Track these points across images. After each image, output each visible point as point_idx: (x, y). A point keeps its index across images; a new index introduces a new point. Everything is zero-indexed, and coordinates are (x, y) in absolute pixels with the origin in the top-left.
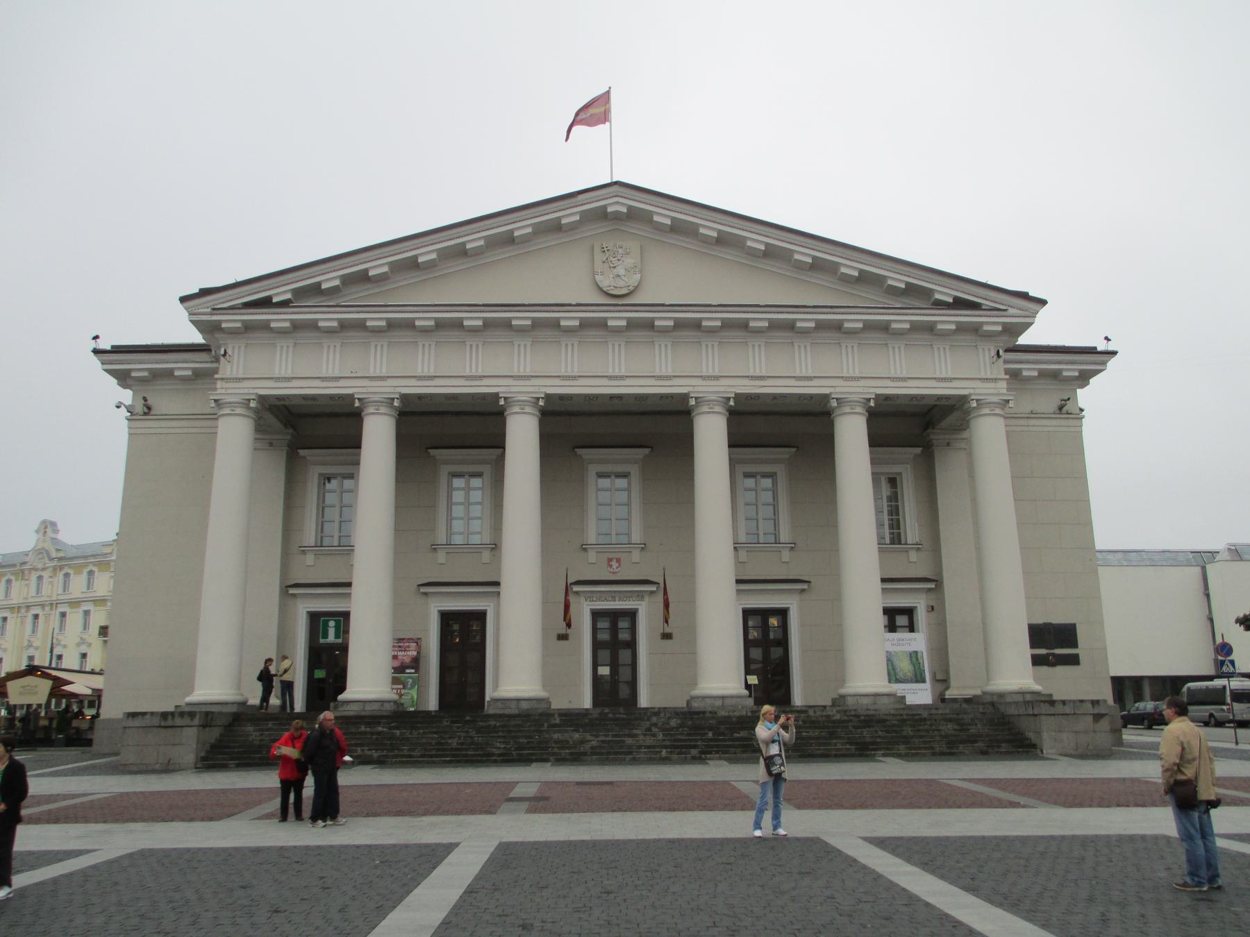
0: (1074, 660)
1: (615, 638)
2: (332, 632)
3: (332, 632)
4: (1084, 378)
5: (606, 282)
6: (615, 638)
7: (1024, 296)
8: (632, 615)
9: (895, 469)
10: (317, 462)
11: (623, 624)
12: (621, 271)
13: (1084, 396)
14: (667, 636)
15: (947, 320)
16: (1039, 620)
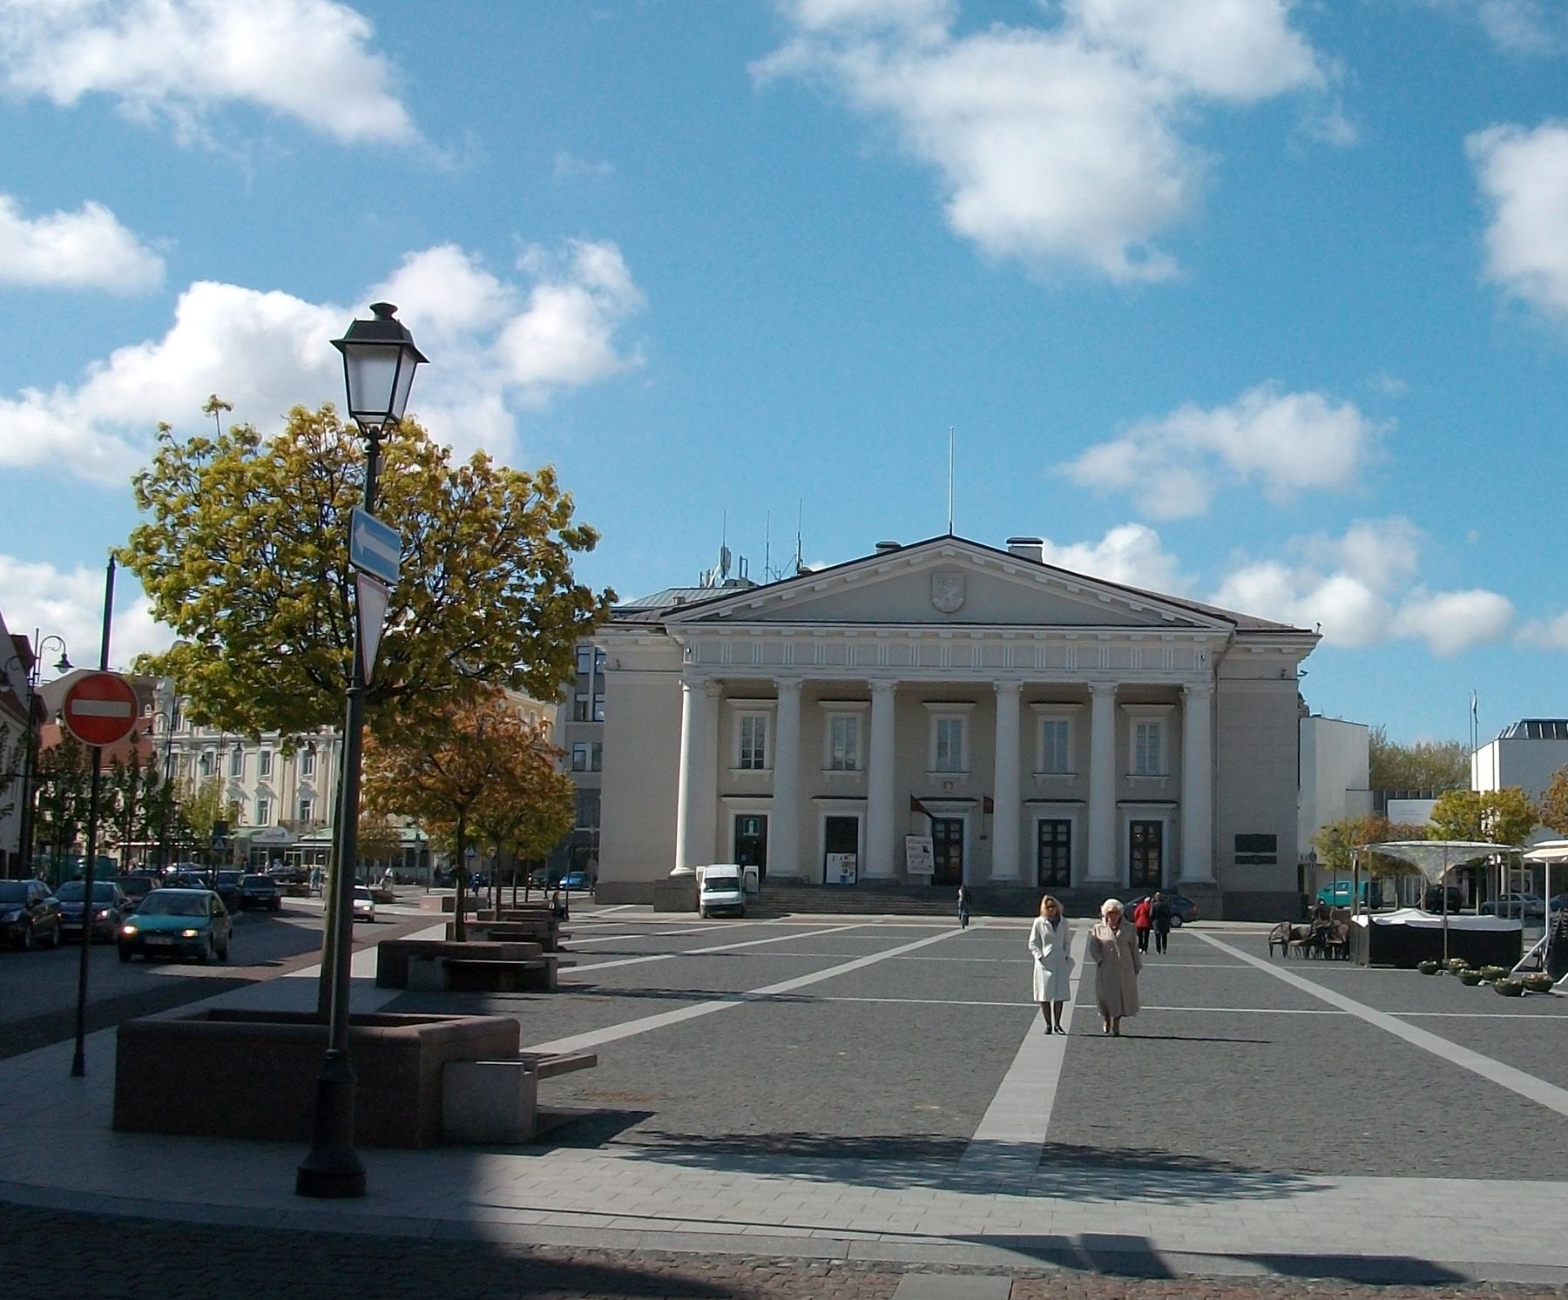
0: (1272, 861)
1: (947, 839)
2: (751, 829)
3: (751, 829)
4: (1303, 653)
5: (940, 604)
6: (947, 839)
7: (1221, 617)
8: (960, 822)
9: (1155, 720)
10: (742, 709)
11: (955, 827)
12: (950, 595)
13: (1300, 667)
14: (984, 837)
15: (1169, 634)
16: (1248, 829)
